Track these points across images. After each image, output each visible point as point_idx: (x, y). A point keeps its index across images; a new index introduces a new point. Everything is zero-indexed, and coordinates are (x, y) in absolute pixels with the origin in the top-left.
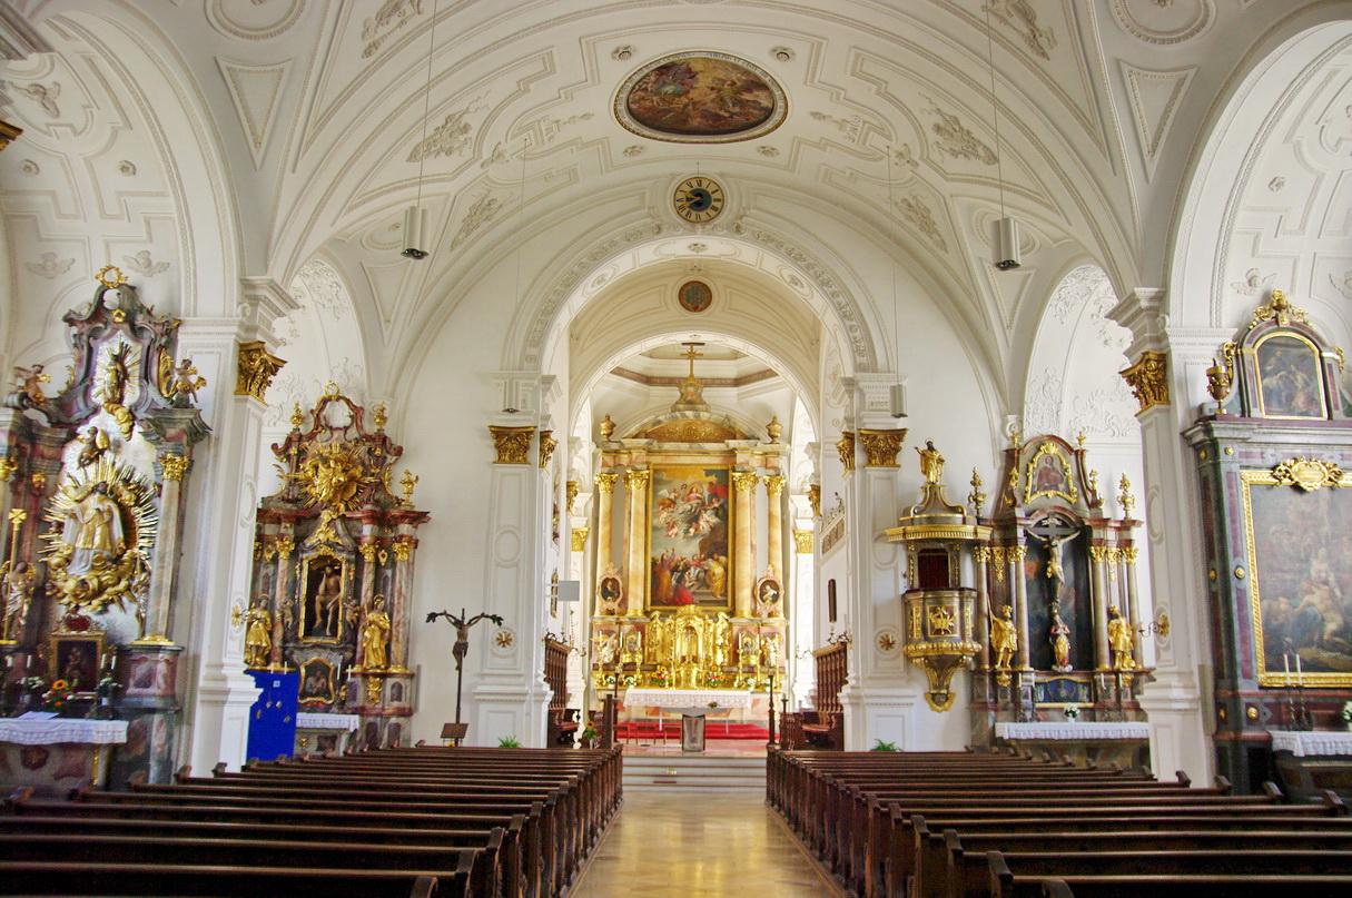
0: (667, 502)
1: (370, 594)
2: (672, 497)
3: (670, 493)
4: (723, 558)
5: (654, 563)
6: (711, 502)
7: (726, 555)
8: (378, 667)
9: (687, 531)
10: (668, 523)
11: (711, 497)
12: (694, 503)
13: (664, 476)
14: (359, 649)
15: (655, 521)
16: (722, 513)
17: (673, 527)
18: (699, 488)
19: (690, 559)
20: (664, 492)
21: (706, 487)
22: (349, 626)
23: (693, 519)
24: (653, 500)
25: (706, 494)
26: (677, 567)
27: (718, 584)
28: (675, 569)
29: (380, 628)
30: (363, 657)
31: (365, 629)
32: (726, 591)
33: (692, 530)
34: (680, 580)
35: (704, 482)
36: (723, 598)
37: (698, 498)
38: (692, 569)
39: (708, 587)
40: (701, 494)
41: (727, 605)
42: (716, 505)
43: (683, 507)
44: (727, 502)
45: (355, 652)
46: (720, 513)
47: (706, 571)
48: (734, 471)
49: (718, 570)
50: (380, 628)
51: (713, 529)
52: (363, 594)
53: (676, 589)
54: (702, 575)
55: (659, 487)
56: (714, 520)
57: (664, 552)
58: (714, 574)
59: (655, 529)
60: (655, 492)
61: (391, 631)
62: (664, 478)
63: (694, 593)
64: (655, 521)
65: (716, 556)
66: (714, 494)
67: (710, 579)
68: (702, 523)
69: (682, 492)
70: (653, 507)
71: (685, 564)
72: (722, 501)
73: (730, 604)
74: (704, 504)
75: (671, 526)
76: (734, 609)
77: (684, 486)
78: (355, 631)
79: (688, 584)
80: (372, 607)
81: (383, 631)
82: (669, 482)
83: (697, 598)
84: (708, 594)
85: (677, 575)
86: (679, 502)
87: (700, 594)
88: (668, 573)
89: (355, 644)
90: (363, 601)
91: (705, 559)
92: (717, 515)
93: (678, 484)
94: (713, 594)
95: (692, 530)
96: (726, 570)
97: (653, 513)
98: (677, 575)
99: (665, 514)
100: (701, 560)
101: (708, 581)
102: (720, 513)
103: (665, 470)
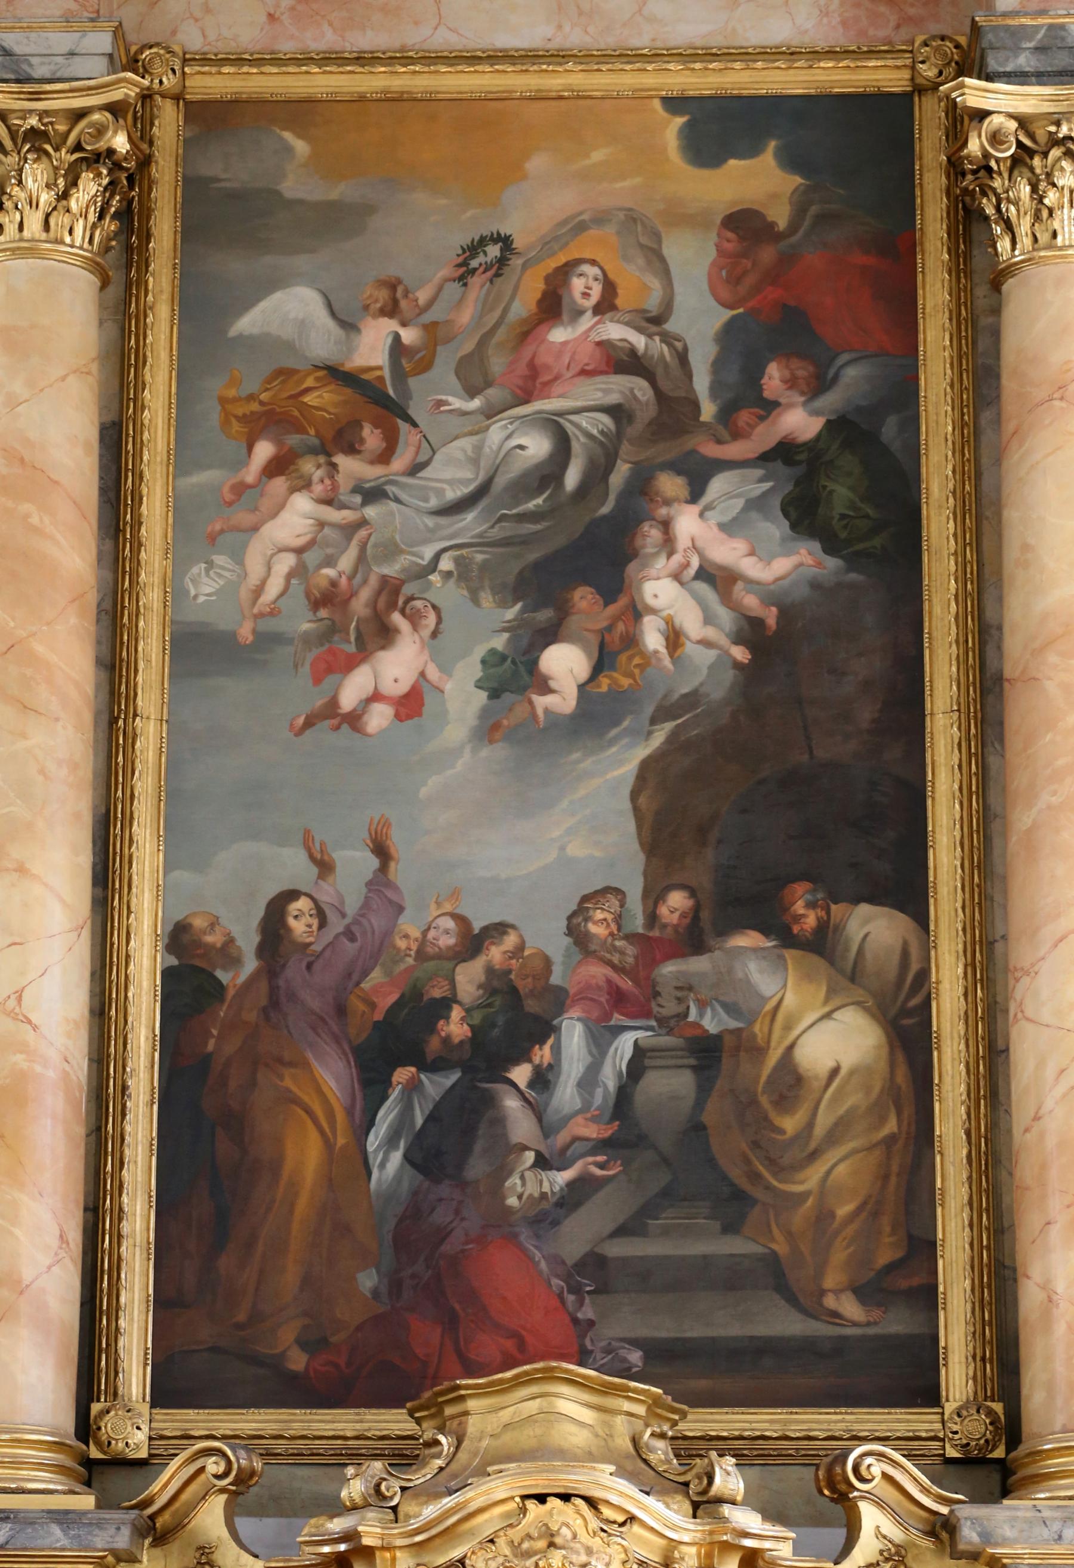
0: (323, 399)
2: (371, 348)
3: (349, 326)
4: (873, 928)
5: (189, 983)
6: (745, 399)
7: (910, 894)
9: (513, 674)
10: (328, 599)
11: (746, 349)
12: (585, 402)
13: (296, 167)
15: (204, 586)
16: (861, 497)
17: (386, 635)
18: (638, 286)
19: (547, 938)
20: (292, 313)
21: (692, 258)
23: (572, 555)
24: (186, 375)
25: (700, 320)
26: (420, 1010)
27: (838, 1175)
28: (393, 1043)
32: (923, 1248)
33: (565, 663)
34: (451, 1143)
35: (681, 217)
36: (897, 1323)
37: (626, 362)
38: (573, 1034)
39: (733, 1206)
40: (653, 321)
41: (929, 1395)
42: (800, 421)
43: (477, 445)
44: (903, 394)
46: (841, 494)
47: (707, 1054)
48: (971, 62)
49: (836, 1042)
51: (772, 644)
53: (412, 1235)
54: (670, 1086)
55: (233, 265)
56: (776, 563)
57: (292, 866)
58: (790, 1083)
59: (198, 650)
60: (203, 312)
62: (293, 186)
63: (595, 1272)
64: (204, 586)
65: (804, 909)
66: (773, 327)
67: (750, 1114)
68: (660, 590)
69: (466, 312)
70: (183, 458)
71: (501, 988)
72: (854, 379)
73: (957, 1379)
74: (674, 413)
75: (354, 620)
76: (1011, 1430)
77: (487, 257)
79: (526, 1185)
82: (336, 221)
83: (627, 1321)
84: (732, 1279)
85: (417, 1092)
86: (440, 395)
87: (645, 1277)
88: (332, 1076)
91: (693, 939)
92: (804, 514)
93: (423, 236)
94: (775, 1277)
95: (565, 663)
96: (909, 1035)
97: (182, 511)
98: (417, 1092)
99: (297, 516)
100: (655, 946)
101: (729, 1148)
102: (841, 494)
103: (300, 112)
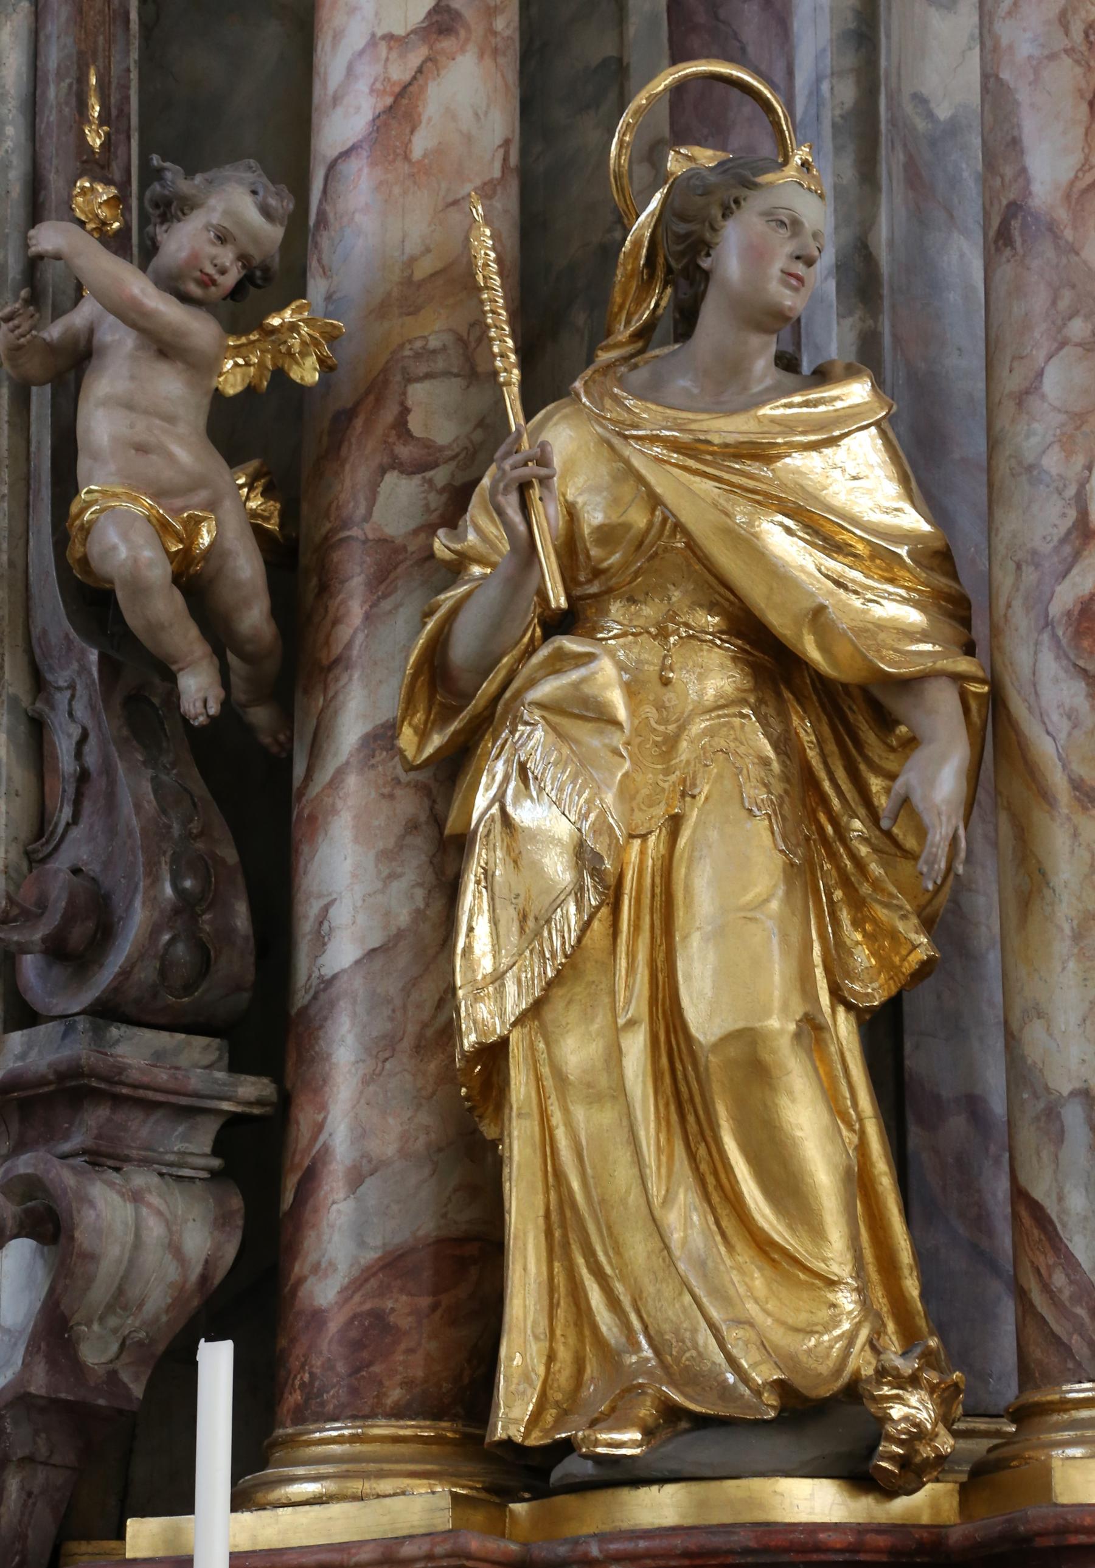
1: (471, 99)
8: (825, 1424)
14: (354, 1110)
22: (135, 678)
29: (770, 661)
30: (465, 1265)
31: (459, 714)
45: (259, 1168)
50: (770, 661)
52: (344, 121)
61: (994, 724)
78: (250, 797)
80: (588, 288)
81: (825, 708)
89: (269, 1027)
90: (371, 223)
